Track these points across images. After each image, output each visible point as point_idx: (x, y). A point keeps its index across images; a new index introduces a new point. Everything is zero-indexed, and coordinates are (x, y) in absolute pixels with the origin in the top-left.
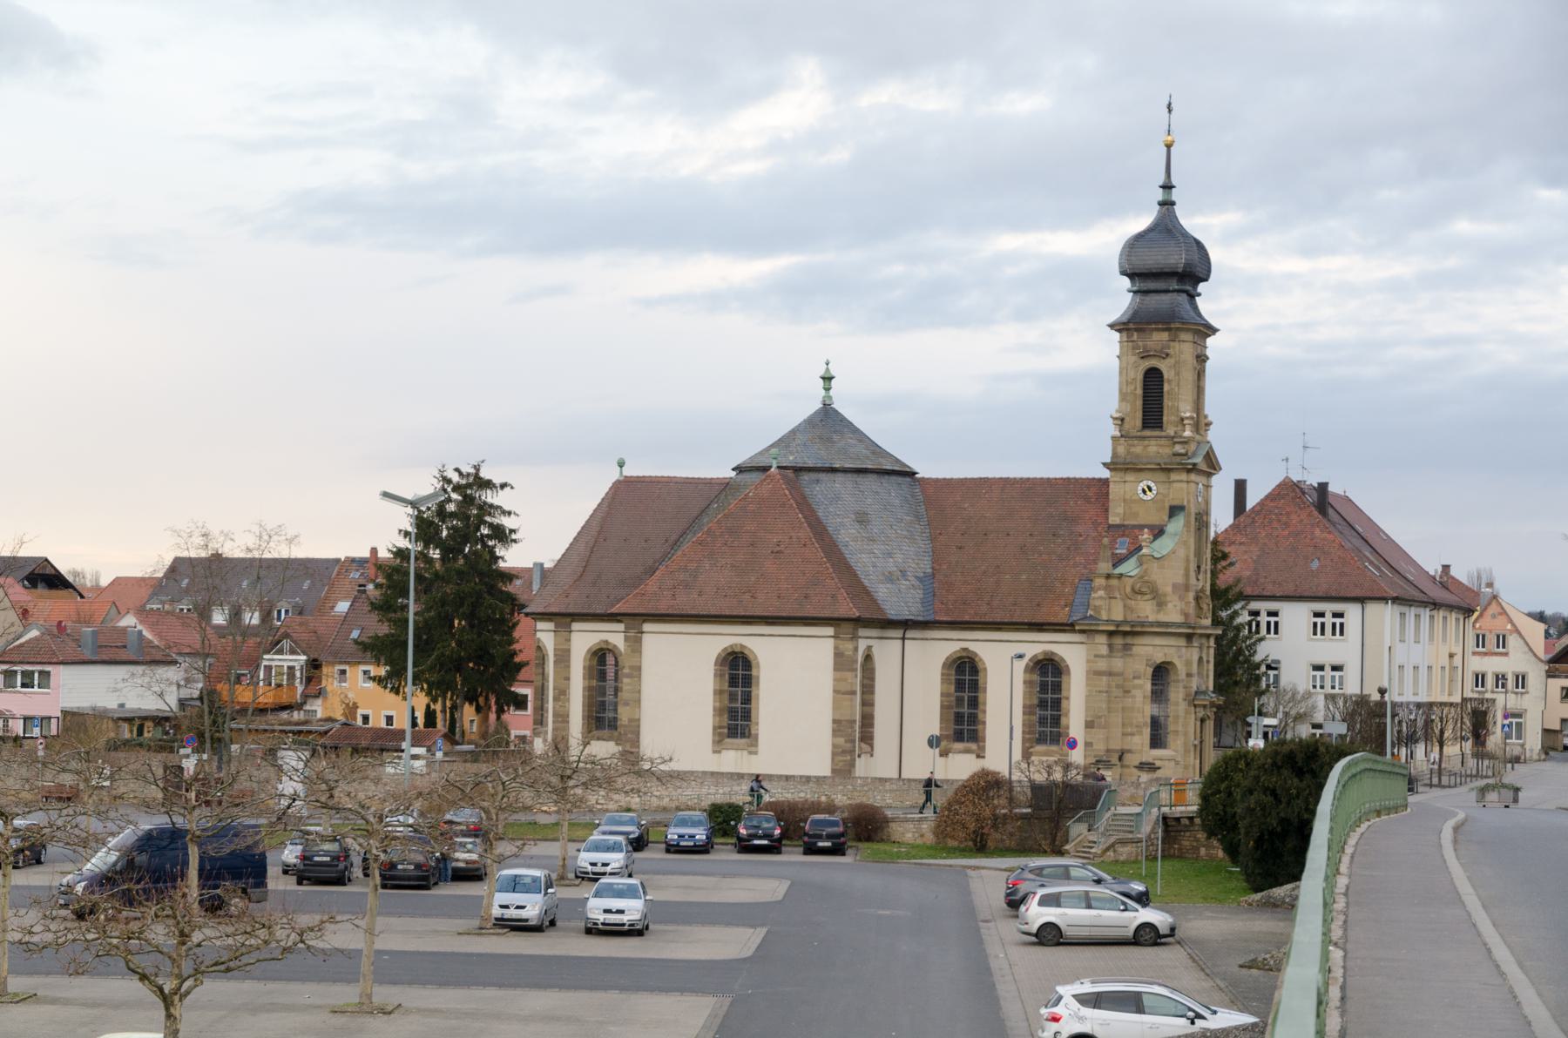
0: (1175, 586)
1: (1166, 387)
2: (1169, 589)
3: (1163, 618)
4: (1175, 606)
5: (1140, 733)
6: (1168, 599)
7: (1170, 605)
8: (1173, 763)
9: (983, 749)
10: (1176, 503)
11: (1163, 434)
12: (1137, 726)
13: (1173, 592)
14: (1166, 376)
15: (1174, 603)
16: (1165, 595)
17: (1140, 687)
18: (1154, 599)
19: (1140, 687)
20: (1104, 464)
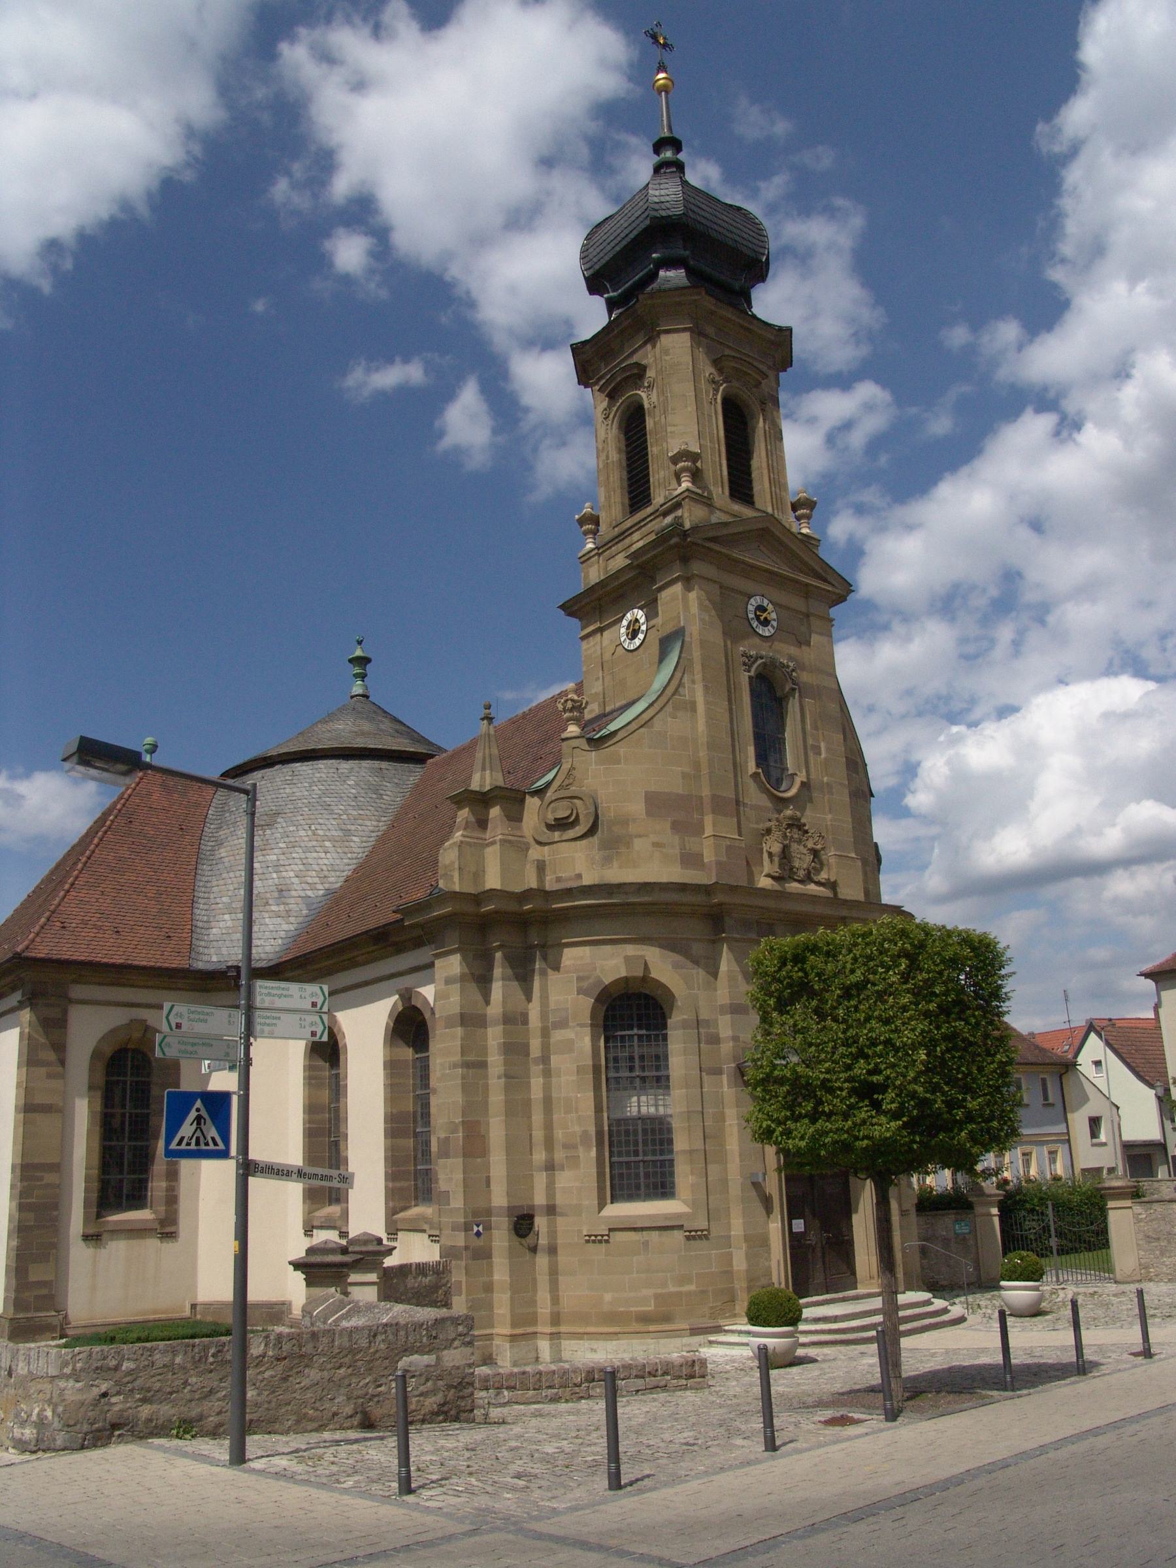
0: (656, 803)
1: (650, 423)
2: (637, 808)
3: (617, 874)
4: (656, 845)
5: (574, 1161)
6: (632, 829)
7: (638, 844)
8: (679, 1235)
9: (345, 1214)
10: (669, 629)
11: (649, 510)
12: (566, 1146)
13: (649, 813)
14: (646, 406)
15: (653, 838)
16: (625, 821)
17: (568, 1046)
18: (592, 831)
19: (568, 1046)
20: (562, 607)
